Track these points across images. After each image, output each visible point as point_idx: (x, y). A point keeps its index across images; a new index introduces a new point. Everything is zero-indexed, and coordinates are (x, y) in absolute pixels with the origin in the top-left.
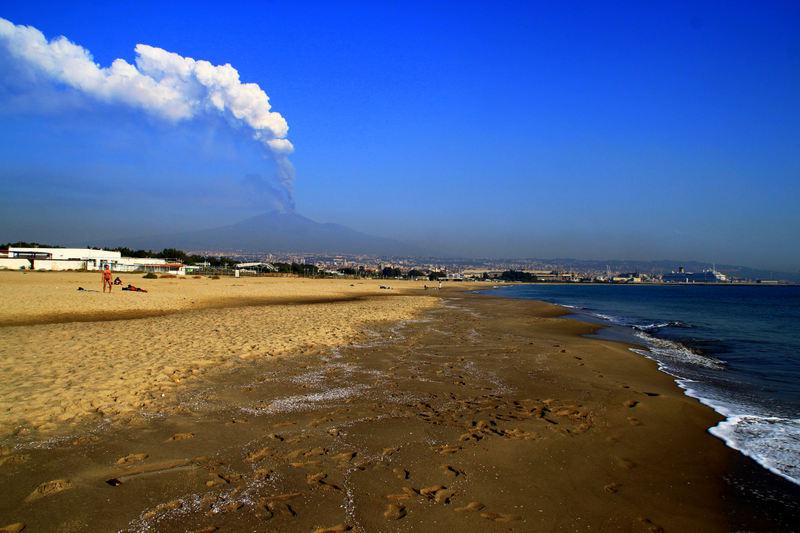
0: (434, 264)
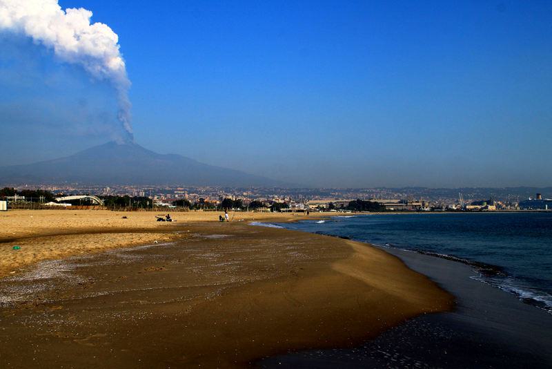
0: (279, 194)
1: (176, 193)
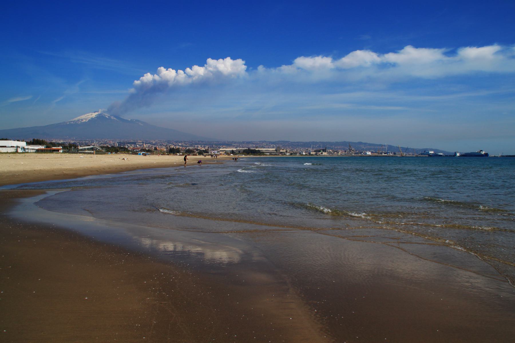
0: (201, 145)
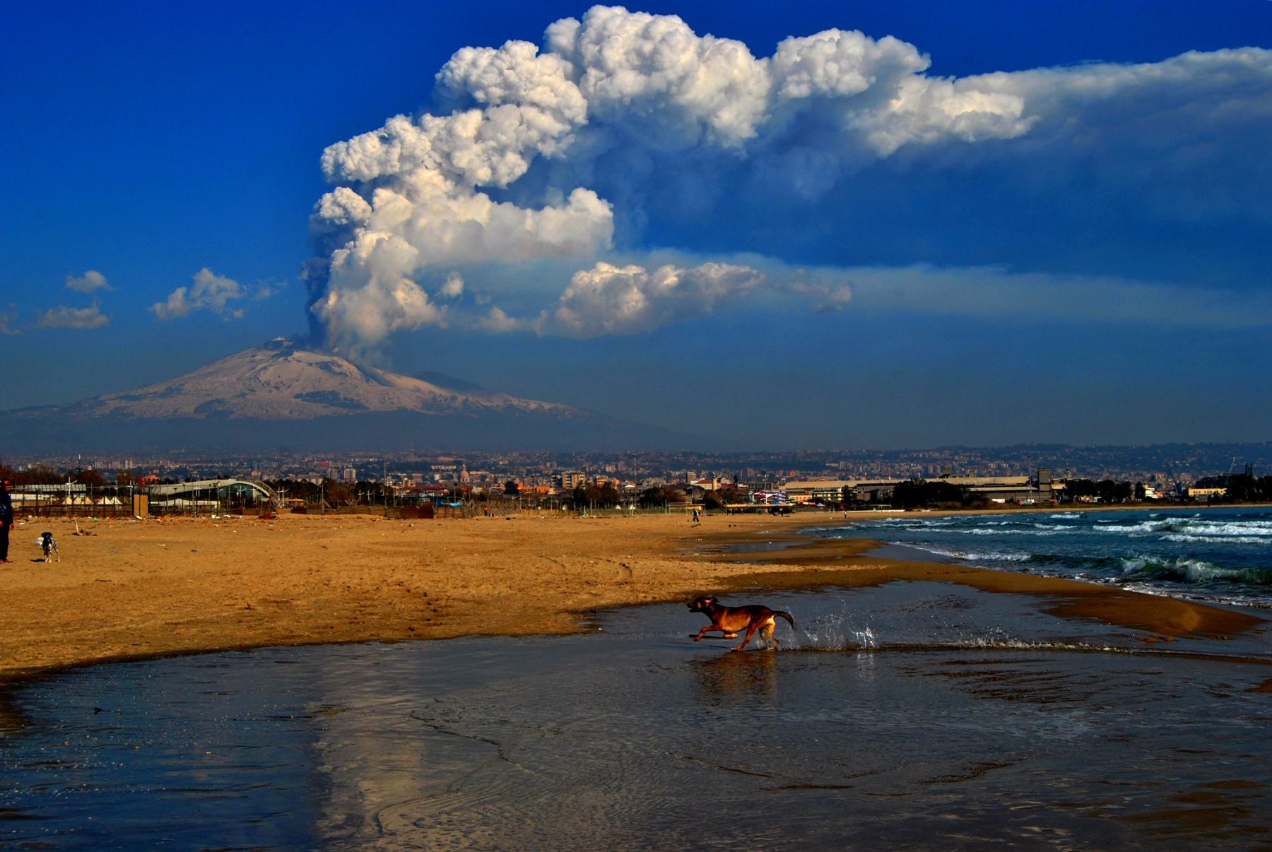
1: (437, 471)
